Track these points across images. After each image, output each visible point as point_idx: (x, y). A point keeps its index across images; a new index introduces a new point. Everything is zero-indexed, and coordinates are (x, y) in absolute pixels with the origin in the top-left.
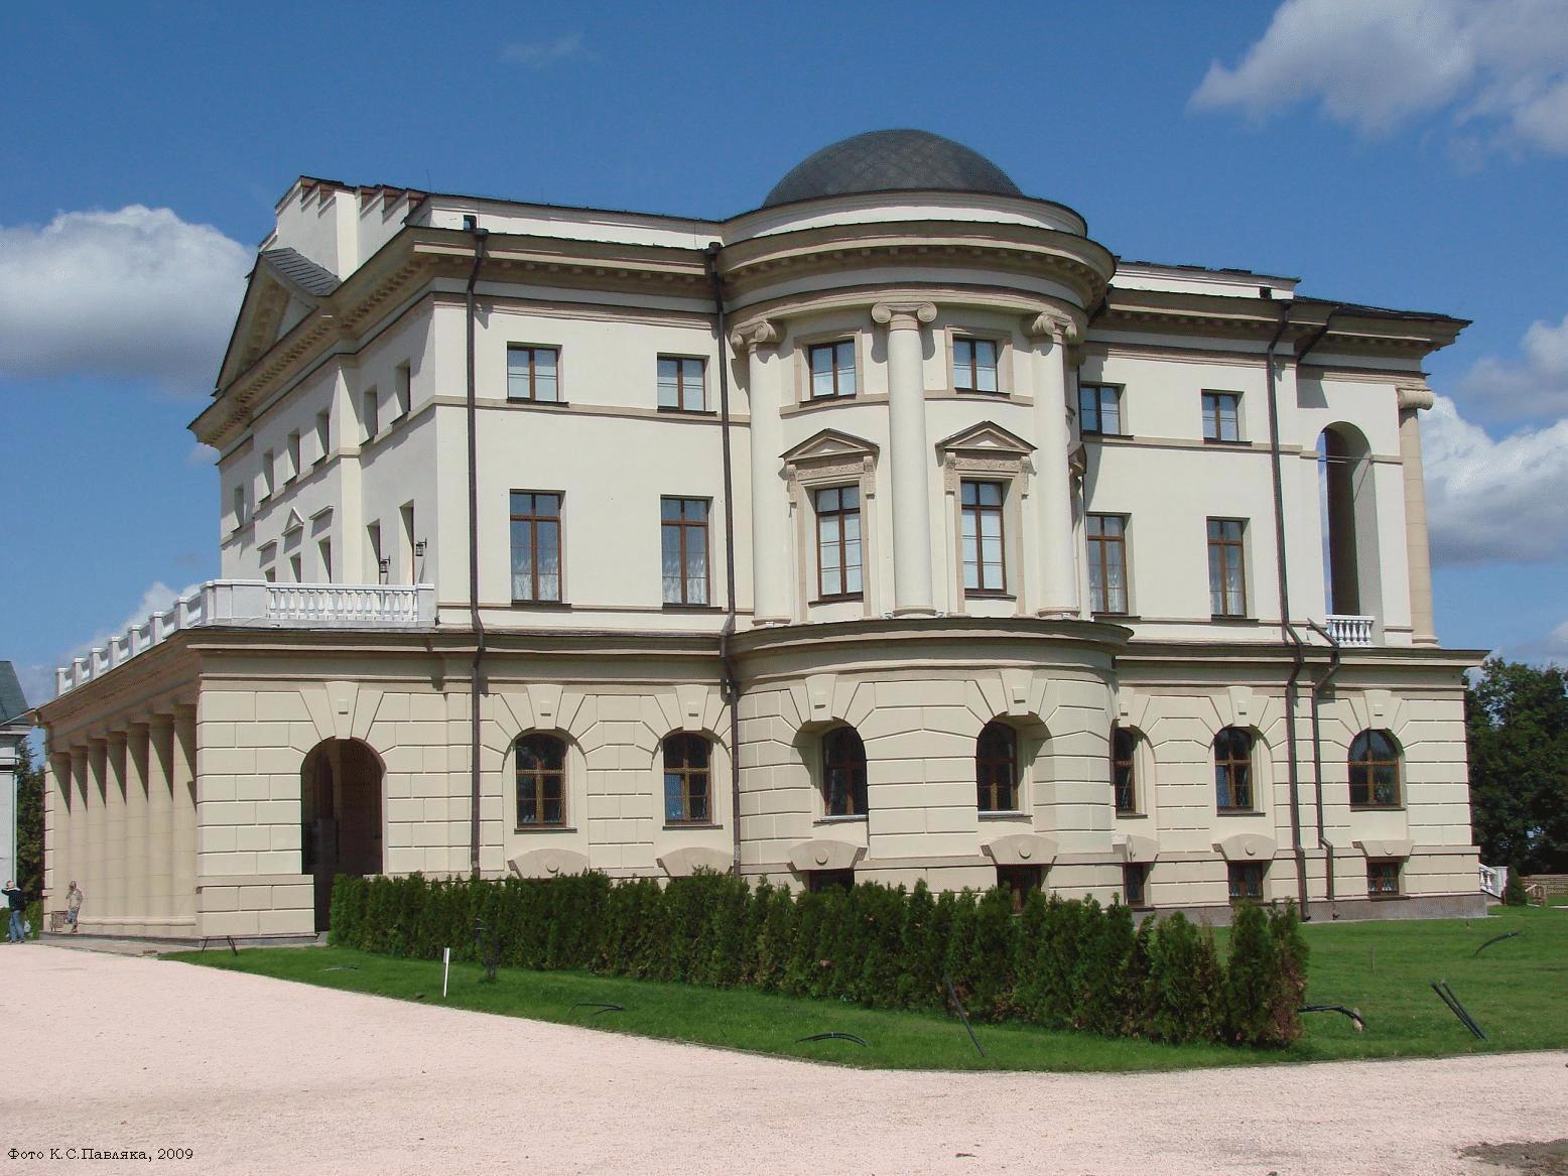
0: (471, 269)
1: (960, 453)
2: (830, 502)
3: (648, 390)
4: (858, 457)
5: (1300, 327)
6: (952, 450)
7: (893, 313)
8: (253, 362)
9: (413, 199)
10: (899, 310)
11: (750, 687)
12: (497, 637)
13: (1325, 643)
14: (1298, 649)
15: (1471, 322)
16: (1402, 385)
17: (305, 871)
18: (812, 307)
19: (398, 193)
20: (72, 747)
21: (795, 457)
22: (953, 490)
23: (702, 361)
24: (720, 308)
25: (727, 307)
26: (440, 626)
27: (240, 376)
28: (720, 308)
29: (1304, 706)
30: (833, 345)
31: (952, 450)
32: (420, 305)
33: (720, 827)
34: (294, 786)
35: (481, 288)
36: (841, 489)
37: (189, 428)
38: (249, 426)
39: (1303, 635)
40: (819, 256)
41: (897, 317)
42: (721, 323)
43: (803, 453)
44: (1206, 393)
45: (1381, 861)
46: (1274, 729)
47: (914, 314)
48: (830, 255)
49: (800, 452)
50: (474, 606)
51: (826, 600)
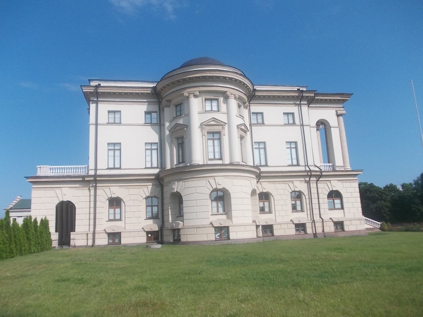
1: (206, 125)
5: (307, 97)
6: (204, 125)
13: (318, 170)
14: (310, 171)
17: (56, 231)
26: (89, 174)
29: (313, 185)
31: (204, 125)
33: (160, 219)
39: (312, 168)
42: (159, 103)
43: (173, 129)
44: (284, 113)
45: (337, 222)
50: (96, 169)
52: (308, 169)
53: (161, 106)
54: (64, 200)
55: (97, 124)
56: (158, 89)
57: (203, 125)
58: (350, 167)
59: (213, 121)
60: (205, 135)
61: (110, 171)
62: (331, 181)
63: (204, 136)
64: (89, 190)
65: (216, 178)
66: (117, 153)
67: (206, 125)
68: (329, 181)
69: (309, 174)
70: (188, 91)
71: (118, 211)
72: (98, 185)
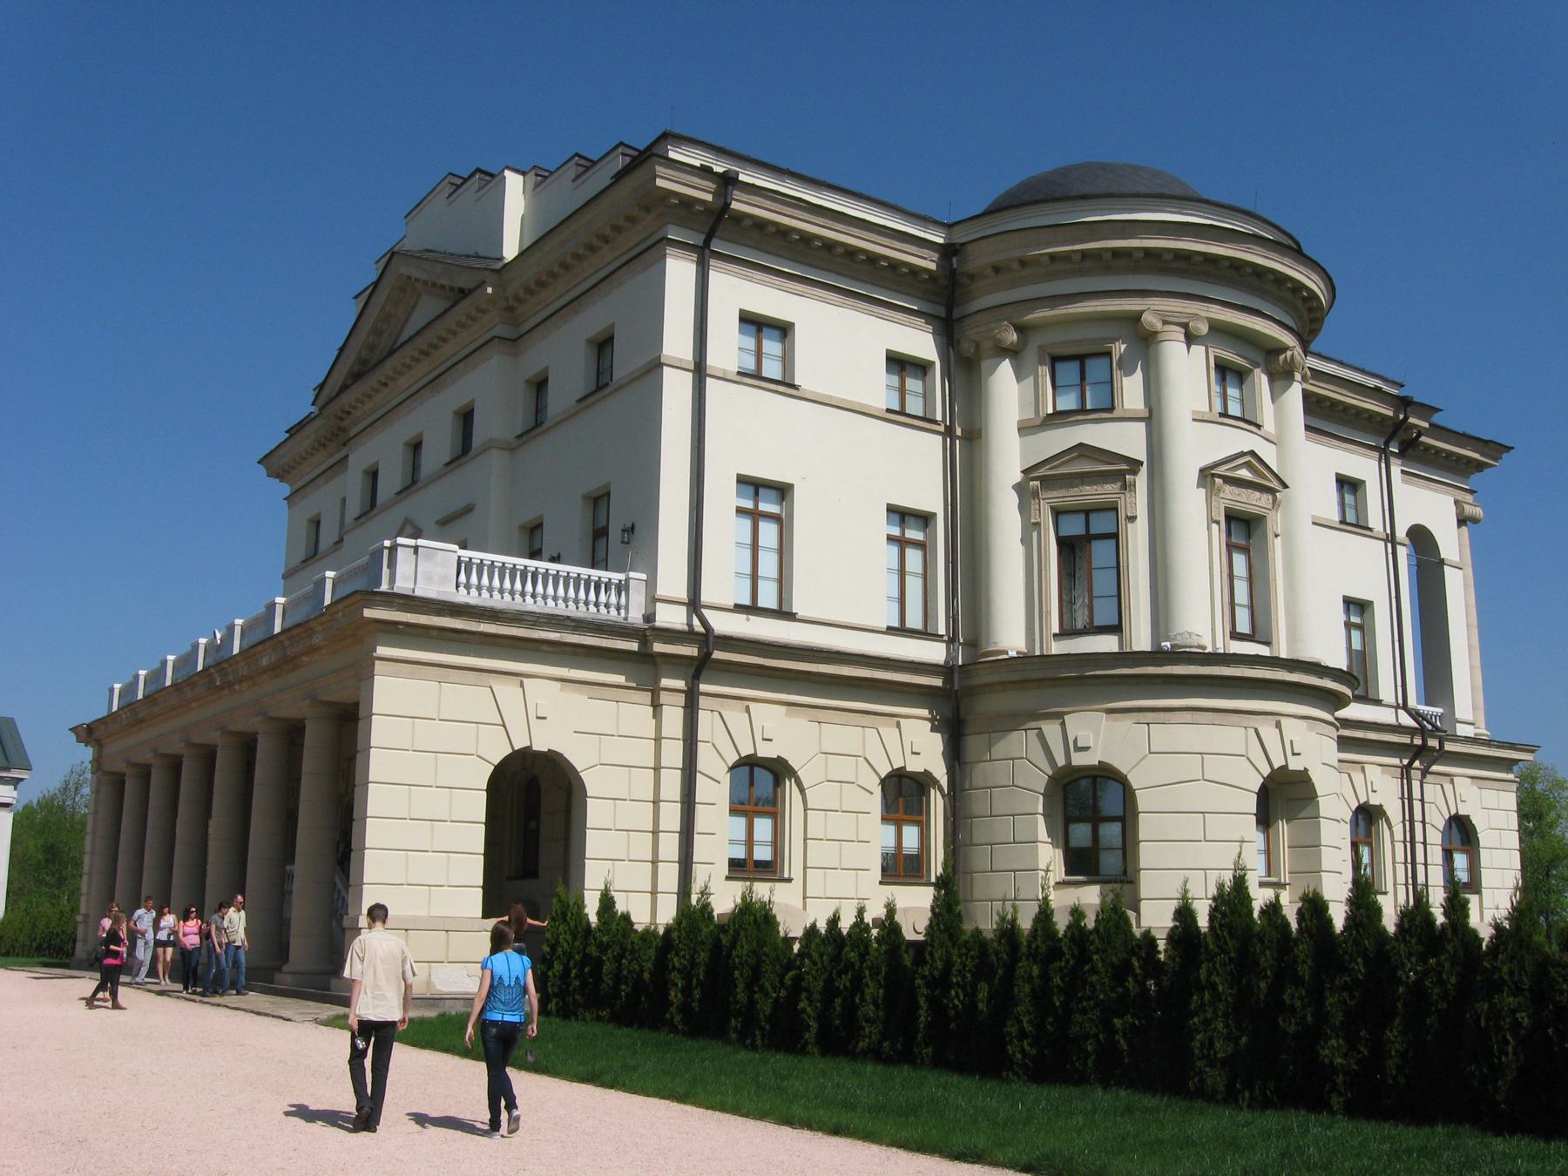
0: (711, 221)
1: (1228, 480)
2: (1074, 527)
3: (878, 389)
4: (1118, 476)
7: (1165, 323)
8: (357, 376)
9: (626, 155)
10: (1171, 319)
11: (1024, 724)
12: (729, 642)
15: (1513, 448)
16: (1460, 498)
18: (1071, 311)
19: (589, 164)
20: (129, 763)
21: (1042, 472)
22: (1218, 519)
23: (920, 367)
24: (950, 309)
25: (956, 315)
27: (344, 388)
28: (950, 309)
30: (1081, 358)
31: (1220, 476)
32: (650, 254)
34: (477, 806)
35: (717, 246)
36: (1087, 512)
37: (258, 462)
38: (344, 445)
40: (1085, 254)
41: (1168, 327)
42: (947, 330)
46: (1394, 810)
47: (1185, 326)
48: (1096, 255)
49: (1048, 467)
50: (694, 603)
51: (1066, 632)
52: (1406, 720)
53: (967, 348)
54: (535, 748)
55: (700, 371)
56: (978, 260)
57: (1213, 475)
58: (1486, 729)
59: (1248, 465)
60: (1218, 523)
61: (748, 620)
62: (1455, 778)
63: (1215, 526)
64: (656, 706)
65: (1284, 722)
66: (768, 532)
67: (1228, 480)
68: (1449, 778)
69: (1418, 741)
70: (1157, 308)
71: (763, 827)
72: (703, 687)
